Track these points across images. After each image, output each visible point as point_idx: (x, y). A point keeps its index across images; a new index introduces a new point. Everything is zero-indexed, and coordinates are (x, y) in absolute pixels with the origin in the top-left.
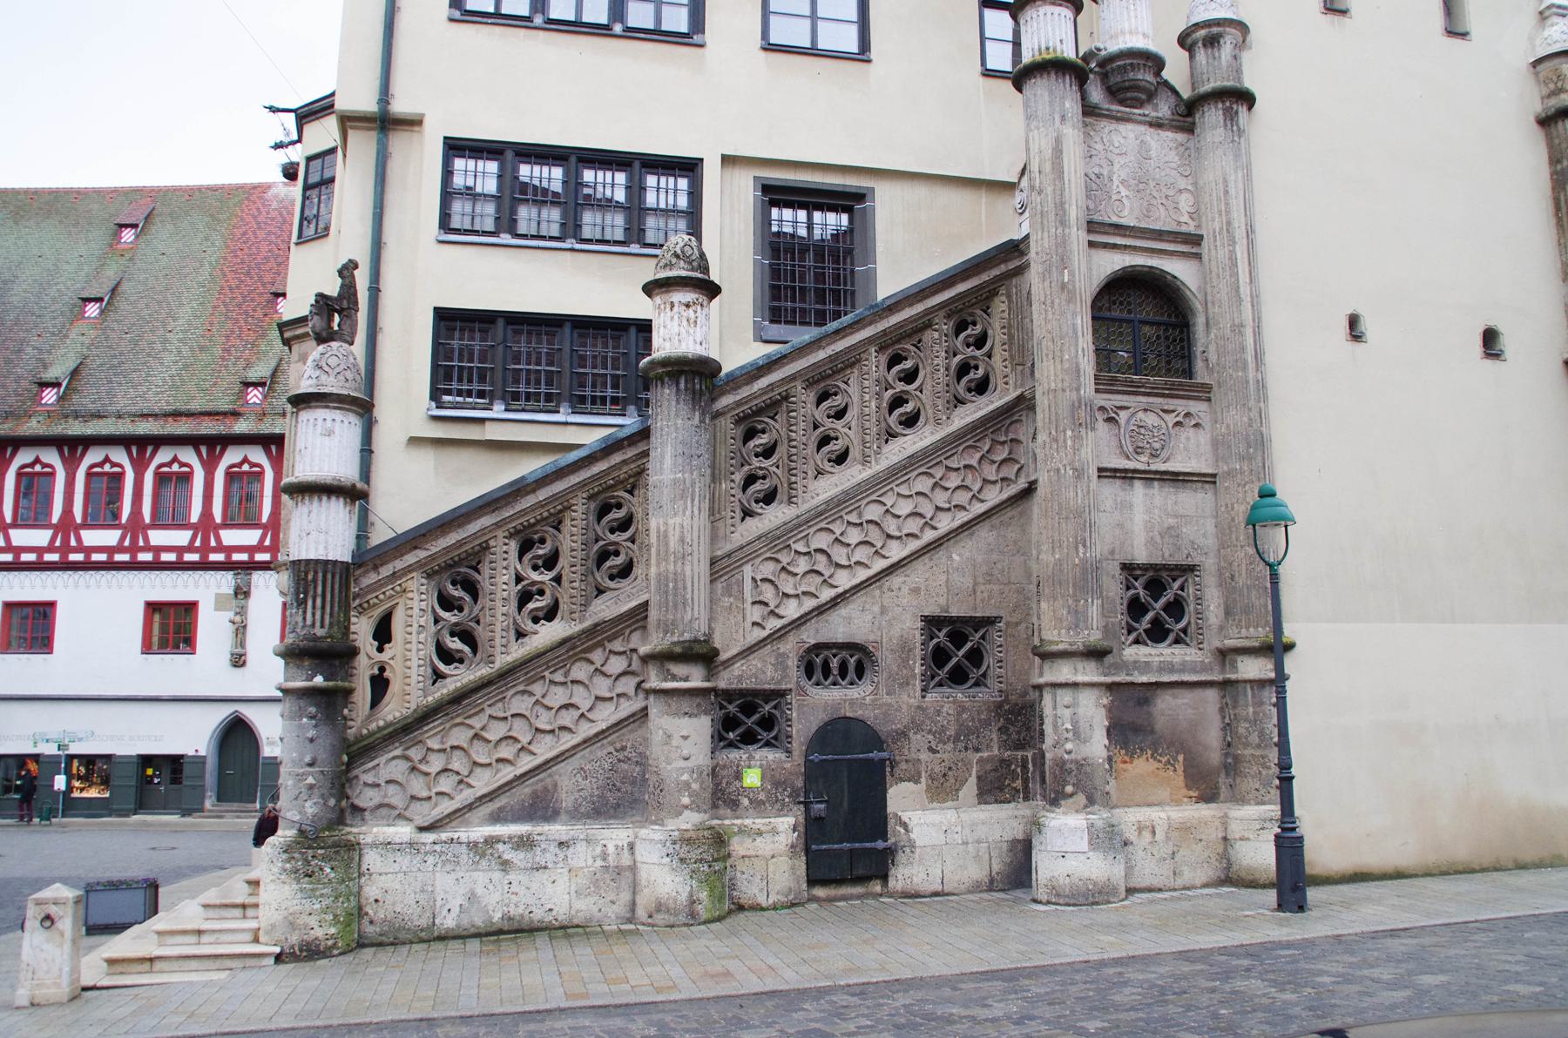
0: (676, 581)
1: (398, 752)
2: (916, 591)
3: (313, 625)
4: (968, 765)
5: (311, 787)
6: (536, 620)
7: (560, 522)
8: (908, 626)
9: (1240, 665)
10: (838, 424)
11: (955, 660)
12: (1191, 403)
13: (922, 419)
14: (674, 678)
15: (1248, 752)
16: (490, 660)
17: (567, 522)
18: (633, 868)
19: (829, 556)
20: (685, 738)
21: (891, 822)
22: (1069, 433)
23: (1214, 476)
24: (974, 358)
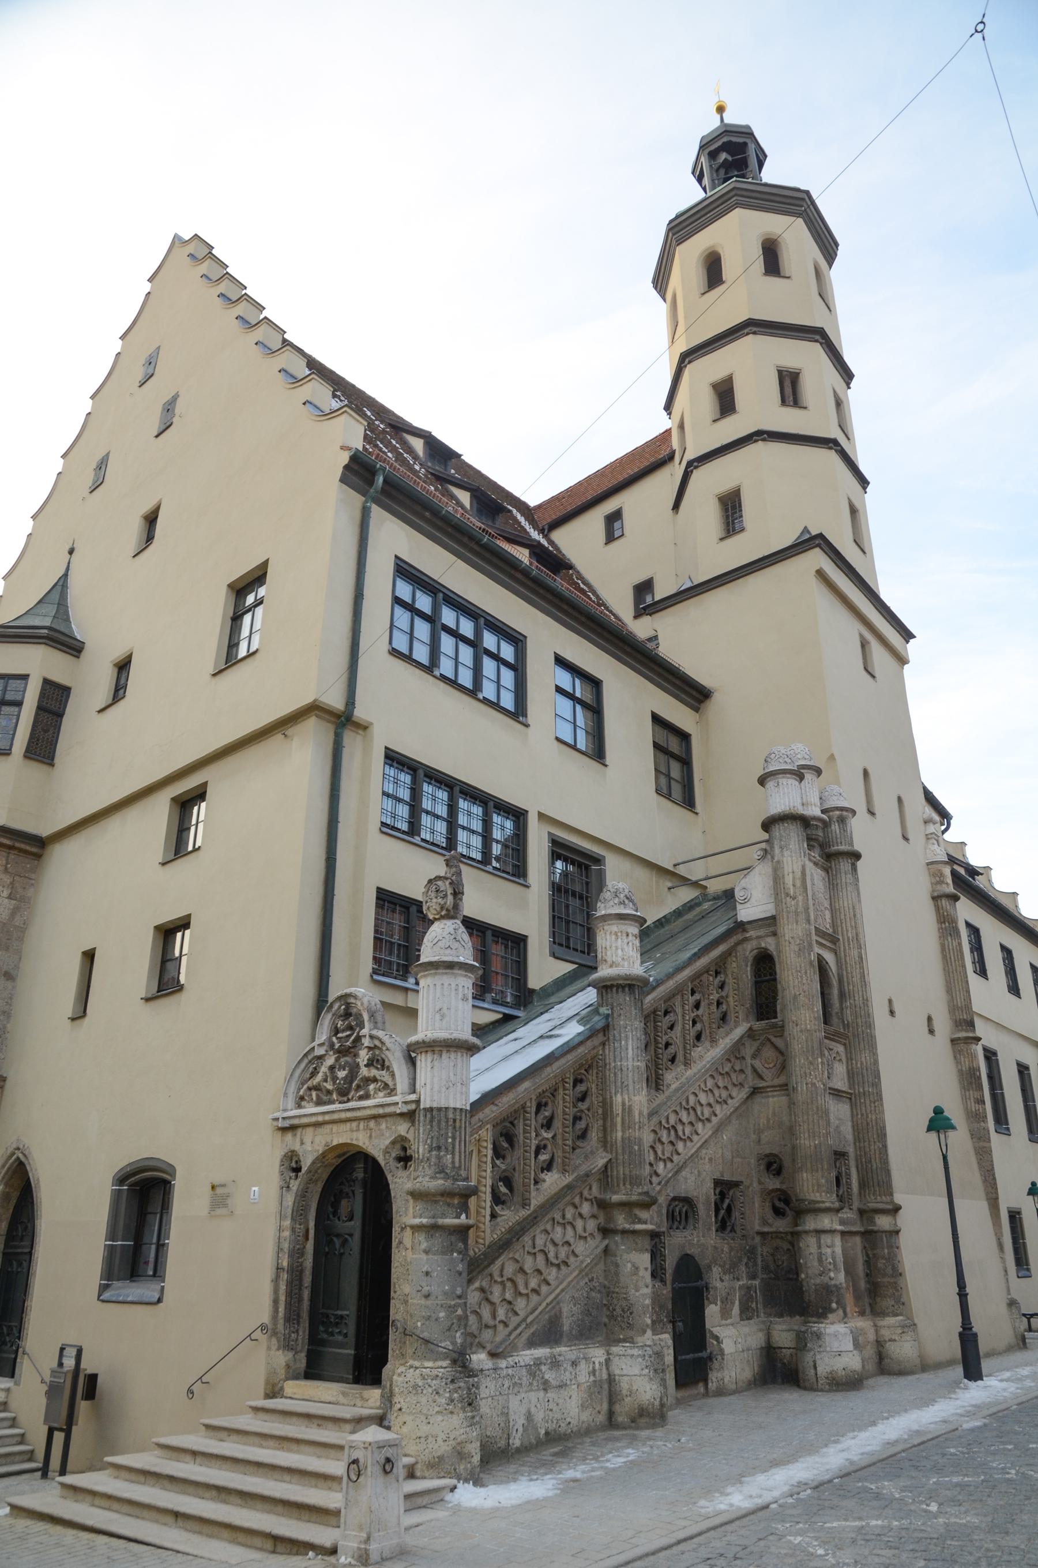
0: (640, 1146)
1: (477, 1284)
2: (710, 1160)
3: (460, 1167)
5: (459, 1318)
6: (542, 1172)
7: (555, 1090)
8: (710, 1184)
9: (877, 1220)
10: (672, 1034)
11: (722, 1212)
12: (838, 1045)
13: (703, 1036)
14: (641, 1221)
15: (886, 1280)
16: (525, 1204)
17: (561, 1091)
18: (611, 1380)
19: (676, 1131)
20: (646, 1269)
23: (851, 1094)
24: (722, 997)
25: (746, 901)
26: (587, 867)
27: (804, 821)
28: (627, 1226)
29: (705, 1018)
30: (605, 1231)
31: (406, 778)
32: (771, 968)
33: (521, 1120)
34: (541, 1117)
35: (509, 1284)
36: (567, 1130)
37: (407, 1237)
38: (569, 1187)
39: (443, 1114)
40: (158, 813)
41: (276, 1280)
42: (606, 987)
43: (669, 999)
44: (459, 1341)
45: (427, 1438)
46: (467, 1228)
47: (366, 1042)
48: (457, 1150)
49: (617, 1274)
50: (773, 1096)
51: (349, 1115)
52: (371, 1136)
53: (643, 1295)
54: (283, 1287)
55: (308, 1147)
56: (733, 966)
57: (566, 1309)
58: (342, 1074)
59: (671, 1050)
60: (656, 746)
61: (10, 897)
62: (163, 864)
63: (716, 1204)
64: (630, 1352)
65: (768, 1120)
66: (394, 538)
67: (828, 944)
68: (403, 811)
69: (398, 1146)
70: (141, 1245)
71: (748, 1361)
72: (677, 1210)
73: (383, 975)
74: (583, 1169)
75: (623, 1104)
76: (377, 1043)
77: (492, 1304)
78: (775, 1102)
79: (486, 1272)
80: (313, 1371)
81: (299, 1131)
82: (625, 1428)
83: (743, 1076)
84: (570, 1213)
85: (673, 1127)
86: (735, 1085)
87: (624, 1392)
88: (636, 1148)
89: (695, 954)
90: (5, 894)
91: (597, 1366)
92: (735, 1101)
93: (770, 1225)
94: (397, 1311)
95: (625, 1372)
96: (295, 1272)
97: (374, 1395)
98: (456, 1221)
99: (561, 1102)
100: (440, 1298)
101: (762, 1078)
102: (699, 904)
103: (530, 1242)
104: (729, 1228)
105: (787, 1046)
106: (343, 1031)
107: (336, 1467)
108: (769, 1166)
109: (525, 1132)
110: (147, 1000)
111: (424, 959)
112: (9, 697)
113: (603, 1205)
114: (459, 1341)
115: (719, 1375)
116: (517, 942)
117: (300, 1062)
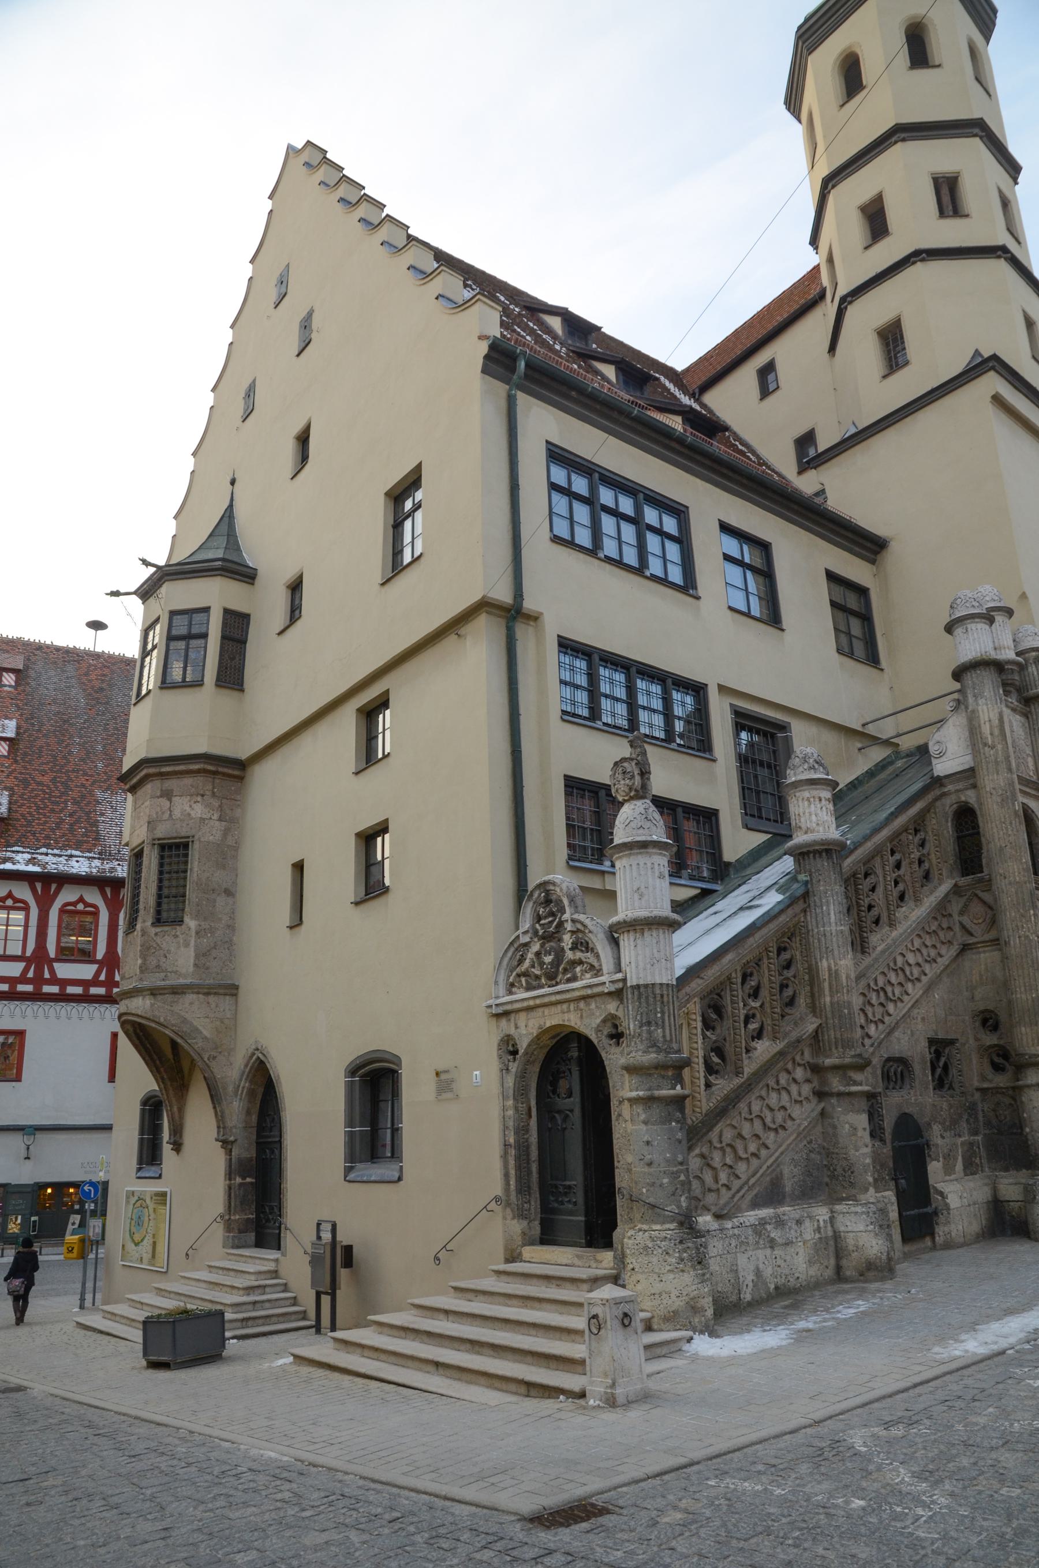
0: (849, 1009)
1: (697, 1151)
2: (923, 1019)
3: (671, 1040)
4: (957, 1147)
5: (683, 1183)
7: (760, 960)
10: (874, 896)
11: (939, 1071)
13: (907, 896)
16: (738, 1072)
17: (765, 961)
18: (837, 1236)
19: (885, 993)
20: (864, 1129)
21: (932, 1191)
22: (1032, 912)
24: (923, 855)
25: (941, 755)
26: (773, 736)
27: (998, 666)
28: (842, 1089)
29: (907, 878)
30: (821, 1095)
31: (581, 664)
32: (973, 822)
33: (728, 992)
34: (747, 987)
35: (728, 1150)
36: (774, 998)
37: (626, 1110)
38: (781, 1054)
39: (650, 990)
40: (345, 725)
41: (505, 1156)
42: (802, 854)
43: (869, 861)
44: (684, 1205)
45: (660, 1294)
46: (684, 1098)
47: (569, 926)
48: (667, 1024)
49: (835, 1135)
50: (984, 952)
51: (559, 997)
52: (582, 1017)
53: (863, 1154)
54: (512, 1162)
55: (523, 1031)
56: (932, 823)
57: (786, 1171)
58: (548, 959)
59: (875, 912)
60: (834, 604)
61: (220, 820)
62: (357, 773)
63: (932, 1062)
64: (853, 1209)
65: (981, 975)
66: (544, 423)
67: (1033, 792)
68: (582, 697)
69: (609, 1024)
70: (377, 1130)
71: (975, 1215)
72: (892, 1070)
73: (579, 861)
74: (794, 1035)
75: (830, 969)
76: (579, 926)
77: (714, 1169)
78: (986, 958)
79: (705, 1139)
80: (548, 1236)
81: (513, 1015)
82: (852, 1282)
83: (952, 933)
84: (783, 1079)
85: (882, 988)
86: (943, 943)
87: (851, 1248)
88: (846, 1011)
89: (892, 813)
90: (216, 817)
91: (822, 1223)
92: (944, 959)
93: (991, 1081)
94: (622, 1179)
95: (850, 1229)
96: (522, 1149)
97: (607, 1257)
98: (672, 1092)
99: (766, 971)
100: (662, 1165)
101: (972, 935)
102: (891, 763)
103: (746, 1109)
104: (947, 1086)
105: (995, 900)
106: (546, 918)
107: (579, 1322)
108: (984, 1022)
109: (733, 1002)
110: (357, 904)
111: (617, 841)
112: (195, 630)
113: (816, 1069)
114: (684, 1205)
115: (946, 1229)
116: (708, 817)
117: (506, 951)
